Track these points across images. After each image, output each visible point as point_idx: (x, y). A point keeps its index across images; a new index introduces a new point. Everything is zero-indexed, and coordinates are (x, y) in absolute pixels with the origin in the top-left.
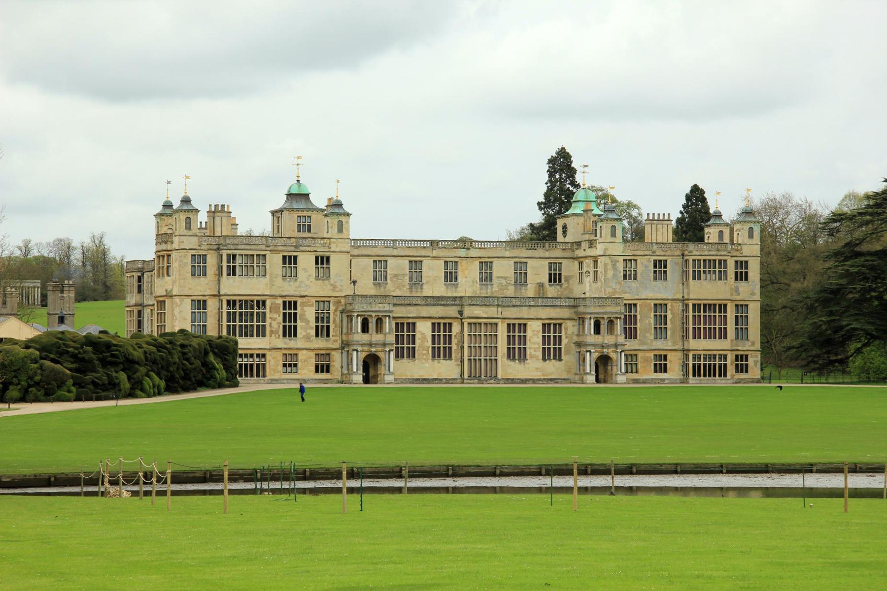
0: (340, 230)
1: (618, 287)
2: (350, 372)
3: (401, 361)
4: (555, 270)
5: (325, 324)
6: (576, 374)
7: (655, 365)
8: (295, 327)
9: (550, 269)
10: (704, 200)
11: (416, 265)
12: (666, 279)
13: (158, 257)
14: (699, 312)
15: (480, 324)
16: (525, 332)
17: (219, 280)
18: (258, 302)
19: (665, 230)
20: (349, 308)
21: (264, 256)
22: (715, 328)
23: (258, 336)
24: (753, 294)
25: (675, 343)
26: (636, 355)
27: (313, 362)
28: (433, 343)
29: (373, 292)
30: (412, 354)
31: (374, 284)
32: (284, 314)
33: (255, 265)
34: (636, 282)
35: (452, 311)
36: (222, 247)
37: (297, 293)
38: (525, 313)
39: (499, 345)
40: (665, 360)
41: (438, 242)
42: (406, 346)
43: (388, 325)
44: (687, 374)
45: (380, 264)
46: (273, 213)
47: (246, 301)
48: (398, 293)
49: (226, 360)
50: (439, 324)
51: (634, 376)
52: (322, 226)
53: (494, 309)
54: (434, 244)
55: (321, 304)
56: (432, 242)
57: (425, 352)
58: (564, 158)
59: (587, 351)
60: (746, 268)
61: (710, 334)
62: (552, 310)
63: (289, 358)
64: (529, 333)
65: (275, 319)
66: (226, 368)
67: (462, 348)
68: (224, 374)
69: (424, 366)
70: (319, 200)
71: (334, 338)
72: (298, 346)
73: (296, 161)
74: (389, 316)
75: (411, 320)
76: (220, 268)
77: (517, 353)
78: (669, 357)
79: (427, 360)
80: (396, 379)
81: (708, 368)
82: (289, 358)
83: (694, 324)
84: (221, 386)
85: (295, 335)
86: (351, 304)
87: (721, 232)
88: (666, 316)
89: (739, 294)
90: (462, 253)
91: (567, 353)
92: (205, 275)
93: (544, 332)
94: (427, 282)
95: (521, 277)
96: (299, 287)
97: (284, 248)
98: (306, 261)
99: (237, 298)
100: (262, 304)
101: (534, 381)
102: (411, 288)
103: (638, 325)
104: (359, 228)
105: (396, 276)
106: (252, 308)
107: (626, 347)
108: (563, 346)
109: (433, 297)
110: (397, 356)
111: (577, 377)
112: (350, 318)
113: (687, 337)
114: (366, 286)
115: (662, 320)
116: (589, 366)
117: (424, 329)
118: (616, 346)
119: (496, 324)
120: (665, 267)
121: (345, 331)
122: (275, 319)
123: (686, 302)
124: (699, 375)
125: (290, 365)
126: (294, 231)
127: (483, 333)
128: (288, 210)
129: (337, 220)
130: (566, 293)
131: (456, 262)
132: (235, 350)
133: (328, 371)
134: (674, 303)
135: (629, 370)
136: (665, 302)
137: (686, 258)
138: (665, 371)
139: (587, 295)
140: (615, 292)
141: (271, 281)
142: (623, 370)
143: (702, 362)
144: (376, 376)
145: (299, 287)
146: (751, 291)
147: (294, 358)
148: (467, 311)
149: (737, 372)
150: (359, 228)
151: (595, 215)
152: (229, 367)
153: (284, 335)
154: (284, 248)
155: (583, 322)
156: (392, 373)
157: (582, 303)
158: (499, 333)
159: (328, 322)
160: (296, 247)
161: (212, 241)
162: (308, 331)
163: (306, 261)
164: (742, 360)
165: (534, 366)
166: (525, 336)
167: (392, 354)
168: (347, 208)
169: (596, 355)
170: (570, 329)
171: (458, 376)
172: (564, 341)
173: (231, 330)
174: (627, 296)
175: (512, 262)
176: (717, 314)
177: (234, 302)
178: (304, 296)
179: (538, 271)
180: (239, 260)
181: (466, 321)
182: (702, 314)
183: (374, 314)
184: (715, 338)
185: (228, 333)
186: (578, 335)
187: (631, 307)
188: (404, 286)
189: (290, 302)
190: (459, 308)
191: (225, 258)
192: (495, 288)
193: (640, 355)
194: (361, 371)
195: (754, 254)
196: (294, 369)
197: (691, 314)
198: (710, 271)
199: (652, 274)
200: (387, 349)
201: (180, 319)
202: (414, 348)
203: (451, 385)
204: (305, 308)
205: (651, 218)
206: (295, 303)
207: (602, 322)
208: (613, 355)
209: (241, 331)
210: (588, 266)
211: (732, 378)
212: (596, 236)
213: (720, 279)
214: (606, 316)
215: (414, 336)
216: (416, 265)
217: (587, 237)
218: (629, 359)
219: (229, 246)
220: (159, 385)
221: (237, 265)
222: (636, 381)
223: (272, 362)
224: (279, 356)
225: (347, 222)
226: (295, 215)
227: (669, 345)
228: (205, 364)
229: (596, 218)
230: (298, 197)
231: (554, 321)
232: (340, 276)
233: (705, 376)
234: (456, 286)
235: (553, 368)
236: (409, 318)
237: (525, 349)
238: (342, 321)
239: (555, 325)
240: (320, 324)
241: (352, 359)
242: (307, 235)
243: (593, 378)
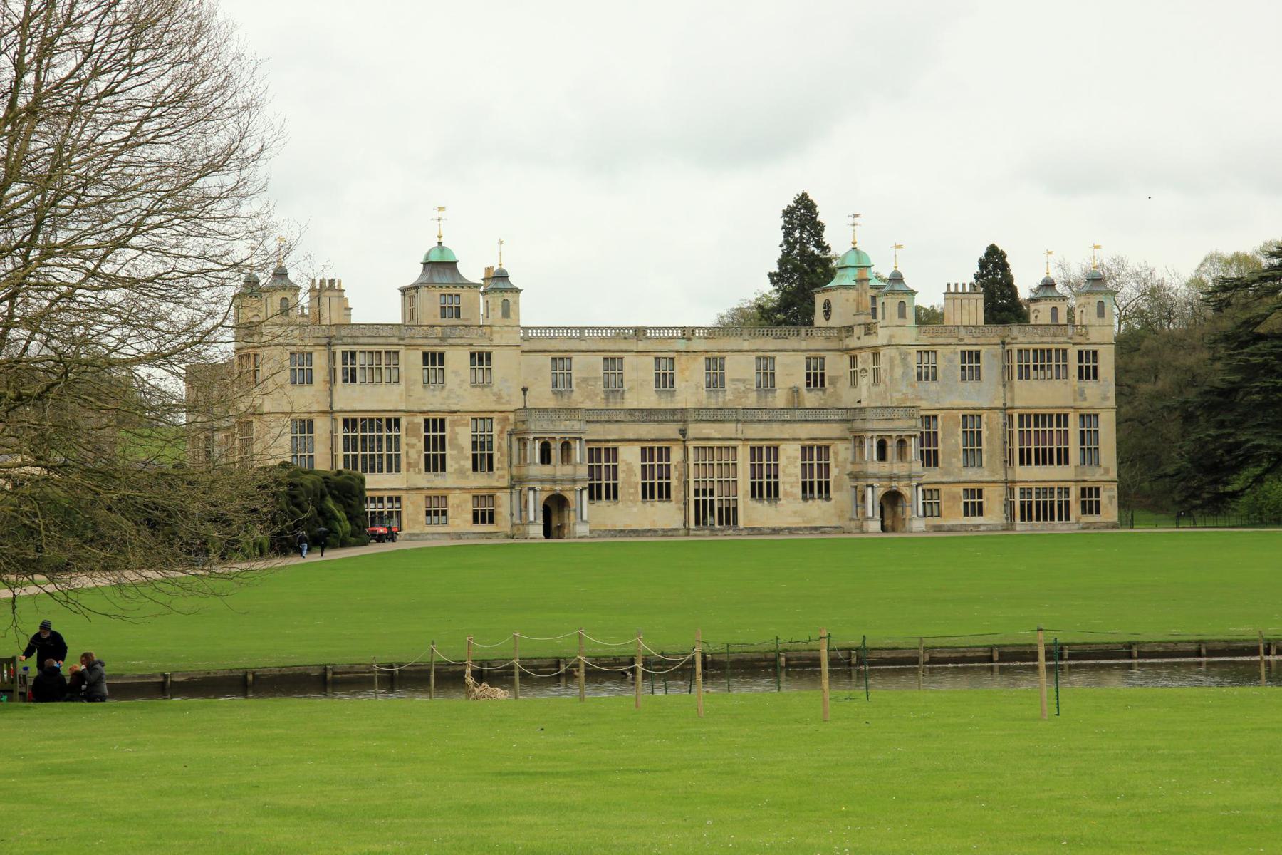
0: (506, 314)
1: (910, 391)
2: (525, 522)
4: (815, 369)
5: (486, 452)
6: (851, 519)
7: (966, 504)
8: (443, 457)
9: (808, 367)
10: (1004, 267)
11: (613, 363)
12: (979, 379)
13: (240, 357)
15: (712, 448)
16: (776, 458)
17: (331, 390)
18: (389, 420)
19: (973, 308)
20: (521, 427)
21: (397, 353)
22: (1051, 450)
23: (390, 470)
24: (1105, 398)
25: (993, 472)
26: (938, 490)
27: (470, 507)
28: (644, 477)
29: (551, 404)
30: (612, 493)
31: (554, 393)
32: (427, 438)
33: (383, 366)
34: (935, 383)
35: (671, 430)
36: (334, 341)
37: (445, 407)
38: (776, 431)
39: (740, 478)
40: (980, 497)
41: (645, 329)
42: (603, 482)
43: (578, 452)
44: (1012, 516)
45: (561, 362)
46: (404, 291)
47: (372, 420)
48: (589, 405)
49: (350, 506)
50: (652, 449)
51: (936, 521)
52: (480, 308)
53: (732, 425)
54: (639, 332)
55: (480, 423)
56: (636, 330)
57: (632, 491)
58: (806, 207)
59: (868, 486)
60: (1095, 361)
61: (1044, 458)
62: (816, 425)
63: (434, 502)
64: (782, 461)
65: (413, 446)
66: (351, 519)
67: (686, 483)
68: (347, 526)
69: (630, 512)
70: (472, 271)
71: (501, 472)
72: (447, 485)
73: (436, 214)
74: (580, 439)
75: (610, 445)
76: (332, 371)
77: (765, 490)
78: (985, 493)
79: (634, 502)
80: (591, 531)
81: (1043, 508)
82: (434, 502)
83: (1022, 443)
84: (344, 544)
85: (443, 469)
86: (524, 422)
87: (1055, 309)
88: (979, 433)
89: (1085, 399)
90: (681, 345)
91: (839, 488)
92: (310, 382)
93: (804, 458)
94: (631, 389)
95: (767, 379)
96: (448, 397)
97: (425, 341)
98: (457, 360)
99: (358, 416)
100: (394, 423)
101: (791, 530)
102: (607, 398)
103: (940, 447)
104: (531, 313)
105: (585, 380)
106: (380, 430)
107: (924, 480)
108: (831, 479)
109: (642, 410)
110: (591, 497)
111: (853, 524)
112: (523, 442)
113: (1012, 463)
114: (542, 395)
115: (973, 439)
116: (871, 507)
117: (630, 457)
118: (910, 477)
119: (735, 448)
121: (515, 461)
122: (413, 446)
123: (1009, 412)
124: (1030, 519)
125: (436, 513)
126: (435, 316)
127: (715, 462)
128: (427, 285)
129: (500, 300)
130: (830, 403)
131: (672, 359)
132: (362, 491)
133: (491, 521)
134: (992, 414)
135: (929, 513)
136: (979, 412)
137: (1008, 347)
138: (981, 514)
139: (864, 404)
140: (906, 397)
141: (407, 389)
142: (921, 513)
143: (1034, 499)
144: (561, 528)
145: (448, 397)
146: (1101, 394)
147: (442, 502)
148: (694, 430)
149: (1084, 512)
150: (531, 313)
151: (872, 287)
152: (355, 516)
153: (427, 470)
154: (425, 341)
155: (862, 443)
156: (586, 522)
157: (859, 416)
158: (739, 462)
159: (490, 448)
160: (442, 339)
161: (319, 332)
162: (462, 463)
163: (457, 360)
164: (1091, 496)
165: (791, 510)
166: (776, 465)
167: (586, 493)
168: (514, 280)
169: (881, 492)
170: (841, 454)
171: (679, 525)
172: (834, 472)
173: (350, 461)
174: (924, 404)
175: (752, 357)
176: (1055, 428)
177: (354, 420)
178: (455, 412)
179: (790, 370)
180: (360, 359)
181: (691, 445)
182: (1033, 429)
183: (558, 437)
184: (1051, 463)
185: (346, 466)
186: (852, 463)
187: (929, 419)
188: (597, 395)
189: (435, 421)
190: (680, 426)
191: (339, 357)
192: (729, 396)
193: (943, 489)
194: (540, 521)
195: (1106, 340)
196: (443, 519)
197: (1016, 429)
198: (1042, 367)
199: (959, 372)
200: (579, 487)
201: (275, 447)
202: (615, 486)
203: (673, 539)
204: (458, 429)
205: (953, 290)
206: (442, 421)
207: (889, 443)
208: (906, 491)
209: (364, 463)
210: (865, 361)
211: (1078, 522)
212: (875, 316)
213: (1058, 377)
214: (894, 434)
215: (615, 467)
216: (613, 363)
217: (862, 319)
218: (928, 496)
219: (345, 340)
220: (261, 544)
221: (357, 366)
222: (938, 529)
224: (420, 498)
225: (517, 302)
226: (437, 293)
227: (983, 474)
228: (321, 512)
229: (873, 292)
230: (440, 268)
231: (819, 443)
232: (506, 381)
233: (1038, 519)
234: (673, 393)
235: (818, 512)
236: (608, 441)
237: (776, 484)
238: (510, 447)
239: (819, 448)
240: (479, 452)
241: (526, 502)
242: (454, 321)
243: (875, 525)
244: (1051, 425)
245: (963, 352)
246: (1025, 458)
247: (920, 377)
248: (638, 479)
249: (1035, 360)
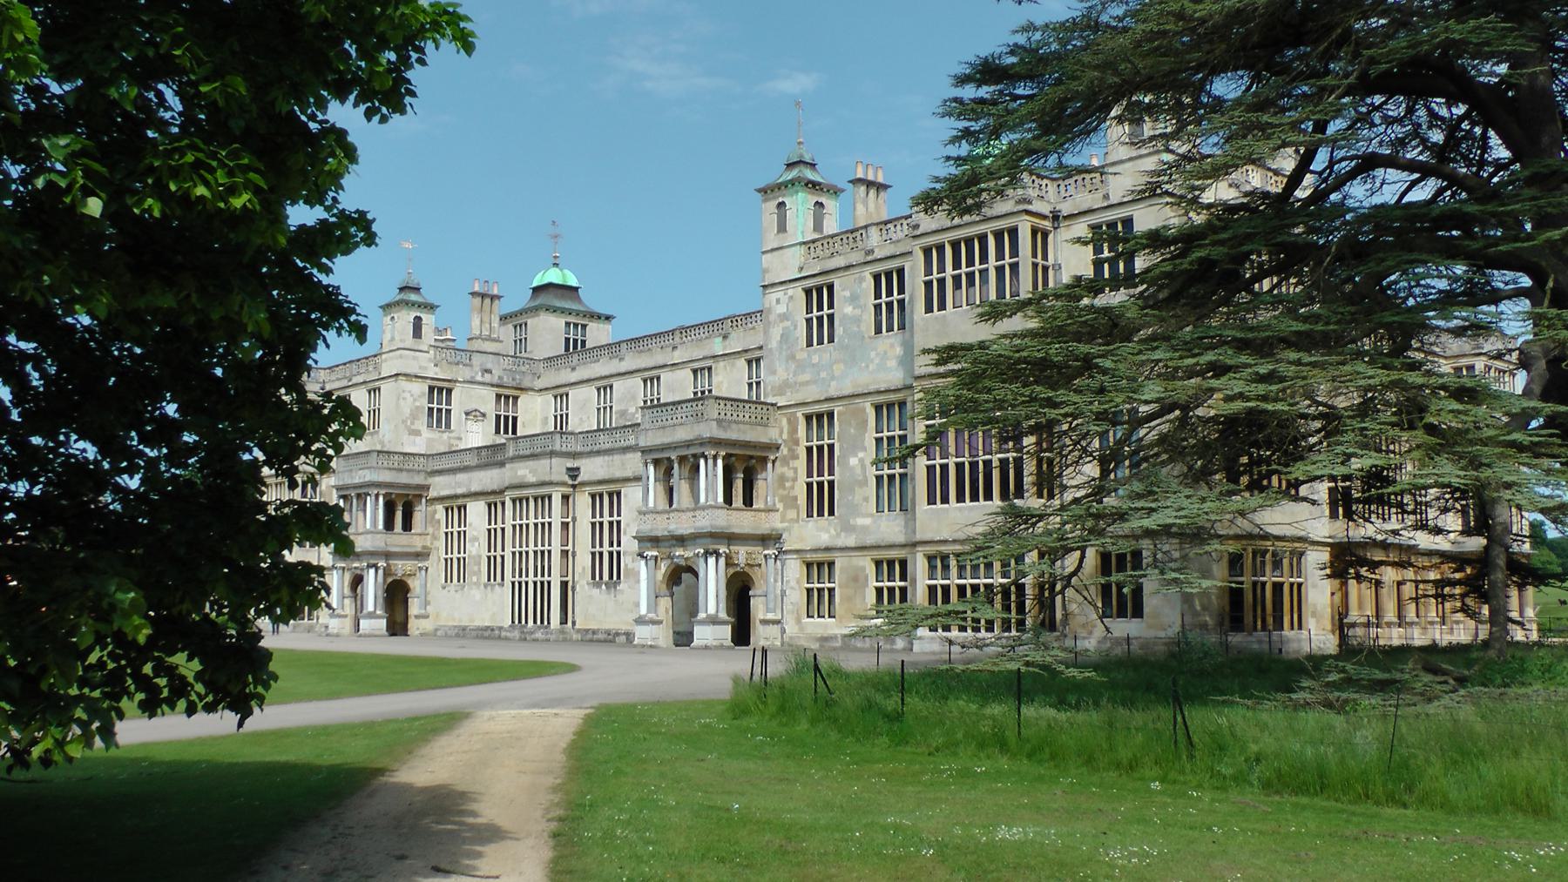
75: (460, 502)
79: (477, 584)
103: (836, 478)
127: (532, 521)
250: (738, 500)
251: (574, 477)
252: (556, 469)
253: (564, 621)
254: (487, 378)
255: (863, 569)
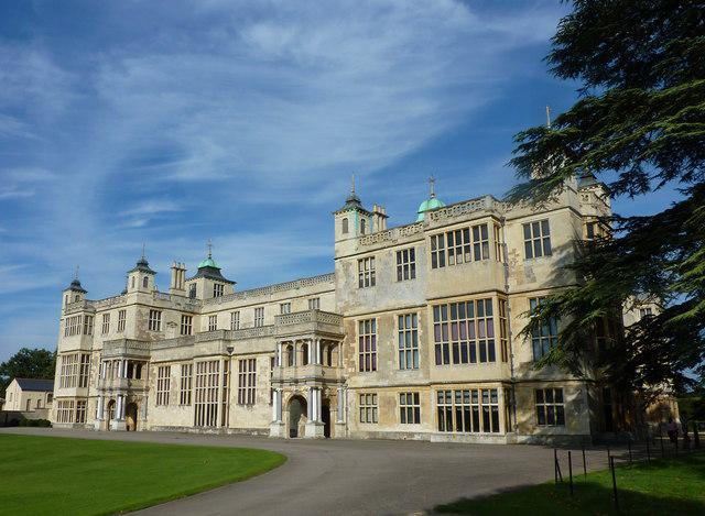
3: (160, 407)
7: (403, 409)
12: (413, 277)
14: (445, 318)
40: (417, 402)
61: (464, 354)
77: (248, 399)
89: (534, 280)
103: (377, 351)
115: (409, 337)
117: (176, 370)
120: (413, 259)
124: (450, 428)
127: (208, 373)
138: (417, 421)
143: (453, 404)
193: (380, 393)
213: (477, 258)
223: (90, 409)
227: (418, 377)
244: (471, 315)
245: (399, 253)
246: (442, 355)
247: (361, 286)
248: (178, 389)
249: (450, 244)
250: (325, 363)
251: (230, 352)
252: (217, 347)
253: (223, 425)
254: (178, 307)
255: (394, 398)
